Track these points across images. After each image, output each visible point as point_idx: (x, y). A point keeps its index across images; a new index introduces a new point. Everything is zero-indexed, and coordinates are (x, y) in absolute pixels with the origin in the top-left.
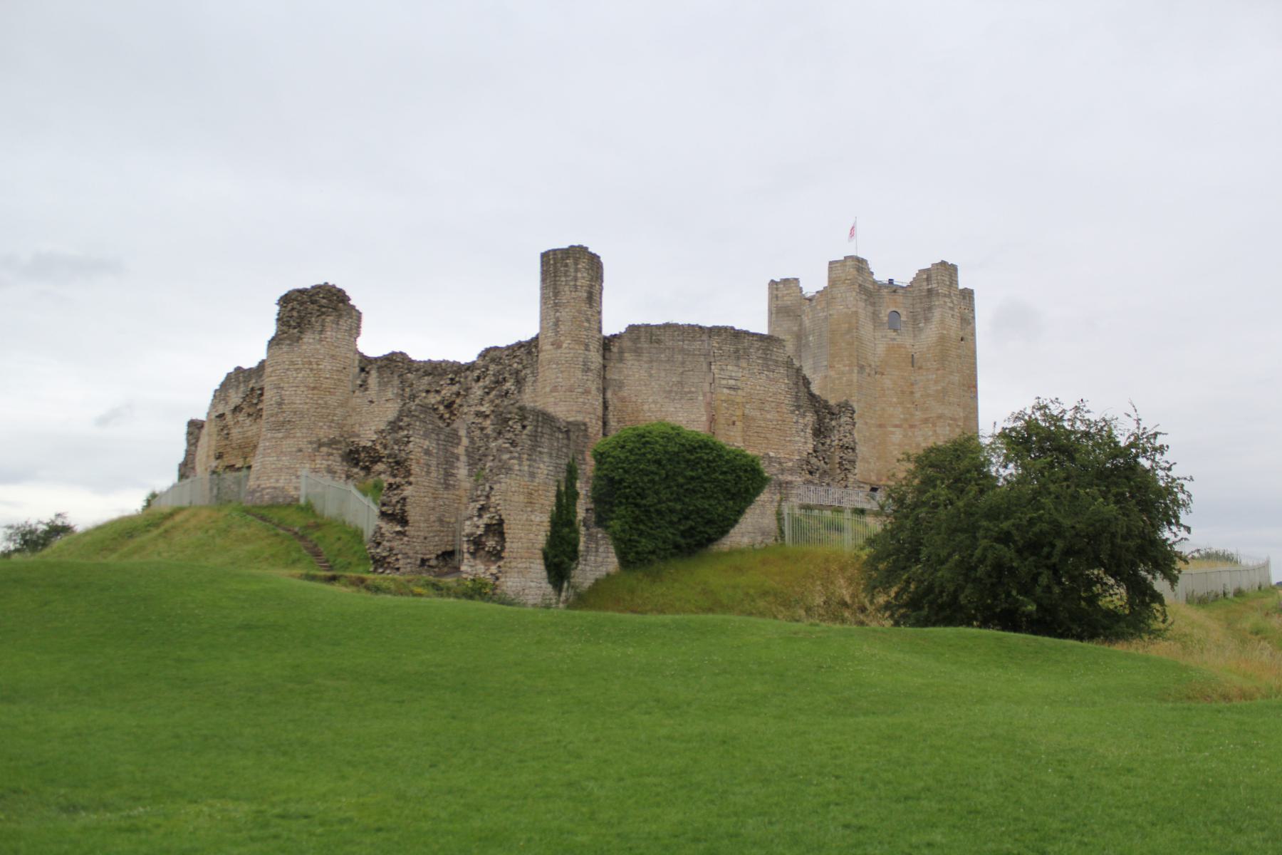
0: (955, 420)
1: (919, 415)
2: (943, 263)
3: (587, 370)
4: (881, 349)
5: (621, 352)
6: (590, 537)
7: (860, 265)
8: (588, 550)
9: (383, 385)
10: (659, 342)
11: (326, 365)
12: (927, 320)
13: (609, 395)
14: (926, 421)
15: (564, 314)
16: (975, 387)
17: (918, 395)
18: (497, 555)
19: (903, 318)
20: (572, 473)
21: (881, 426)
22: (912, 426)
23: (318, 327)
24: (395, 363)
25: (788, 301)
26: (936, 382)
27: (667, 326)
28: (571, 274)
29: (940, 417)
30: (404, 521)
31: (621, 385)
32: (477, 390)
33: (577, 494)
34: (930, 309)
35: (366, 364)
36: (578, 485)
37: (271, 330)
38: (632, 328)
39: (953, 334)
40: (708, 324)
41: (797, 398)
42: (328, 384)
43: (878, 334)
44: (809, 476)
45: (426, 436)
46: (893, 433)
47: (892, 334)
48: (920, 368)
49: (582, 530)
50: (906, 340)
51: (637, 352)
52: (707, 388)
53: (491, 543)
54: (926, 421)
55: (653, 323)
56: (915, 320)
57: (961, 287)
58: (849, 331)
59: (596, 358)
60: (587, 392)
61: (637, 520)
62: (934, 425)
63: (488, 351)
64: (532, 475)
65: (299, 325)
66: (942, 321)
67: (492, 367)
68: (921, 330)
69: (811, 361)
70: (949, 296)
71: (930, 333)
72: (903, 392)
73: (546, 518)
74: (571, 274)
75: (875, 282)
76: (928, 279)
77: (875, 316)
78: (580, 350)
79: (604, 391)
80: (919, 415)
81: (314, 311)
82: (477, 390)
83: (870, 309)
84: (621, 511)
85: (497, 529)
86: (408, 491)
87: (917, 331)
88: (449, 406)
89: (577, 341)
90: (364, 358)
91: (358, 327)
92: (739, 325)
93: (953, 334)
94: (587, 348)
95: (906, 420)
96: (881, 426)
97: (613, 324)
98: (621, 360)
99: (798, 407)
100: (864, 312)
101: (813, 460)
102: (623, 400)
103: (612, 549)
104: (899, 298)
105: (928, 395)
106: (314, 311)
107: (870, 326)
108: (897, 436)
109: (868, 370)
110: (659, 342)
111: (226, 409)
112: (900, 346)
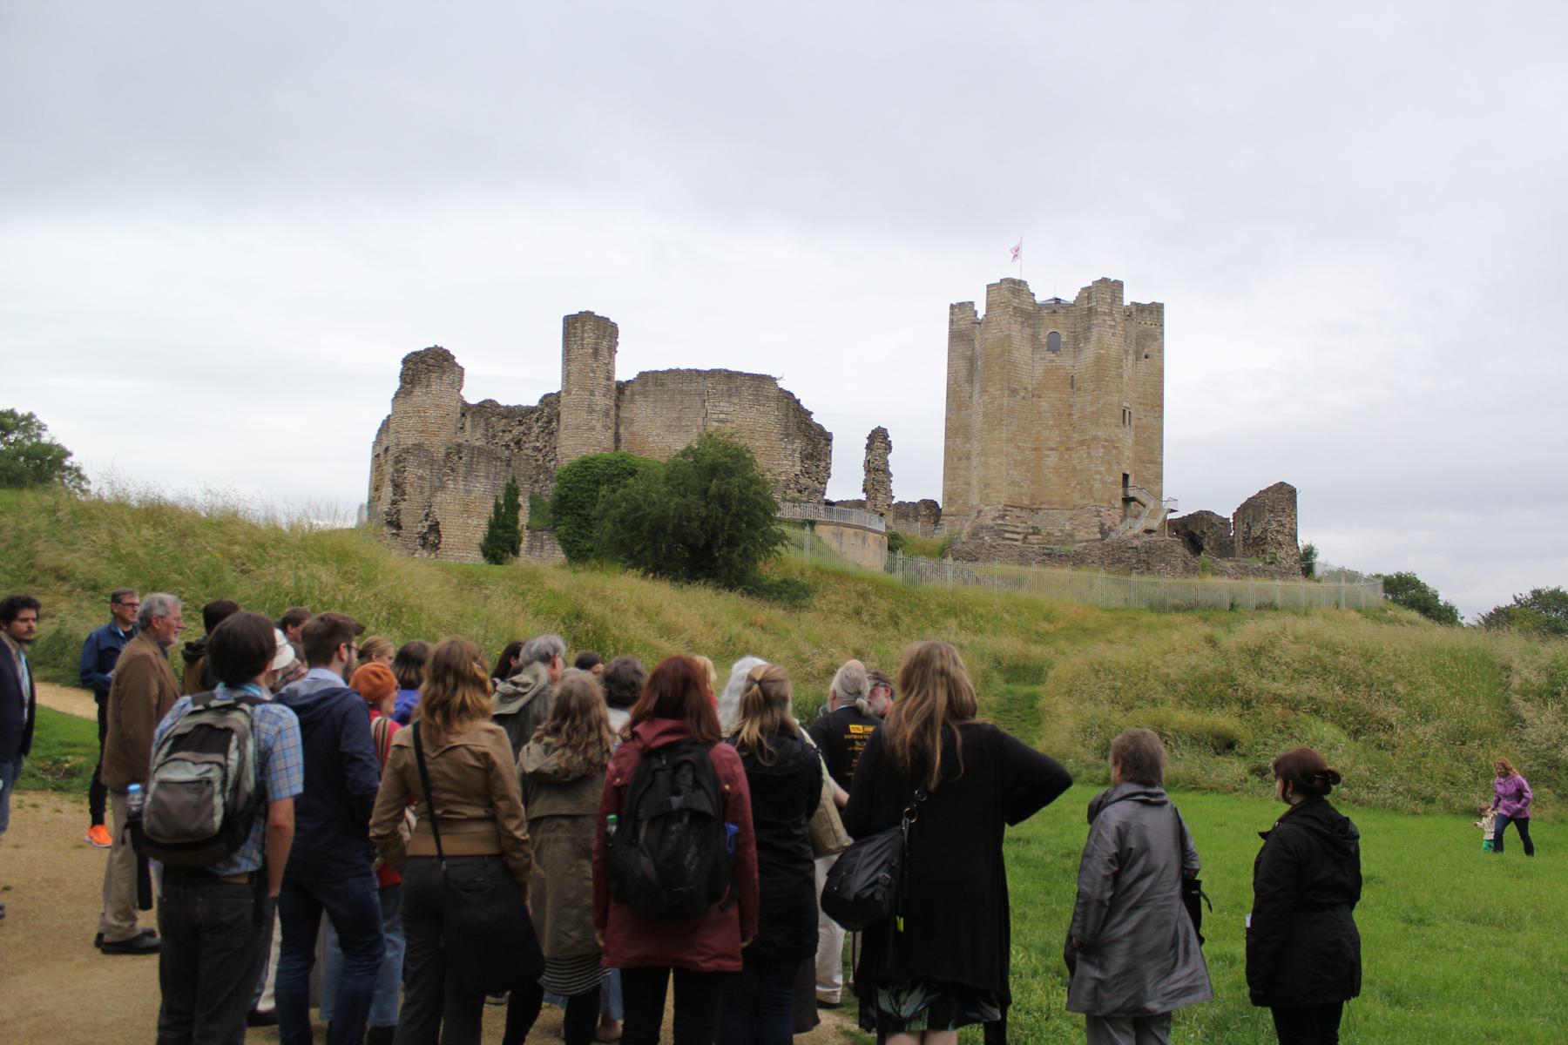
0: (1112, 441)
2: (1104, 280)
3: (591, 410)
4: (1039, 371)
5: (633, 395)
6: (534, 537)
7: (1017, 287)
8: (531, 548)
9: (474, 426)
10: (663, 385)
11: (432, 413)
12: (1087, 339)
13: (622, 430)
14: (1082, 443)
15: (574, 368)
16: (1161, 406)
18: (436, 547)
19: (1064, 339)
20: (512, 492)
21: (1036, 449)
22: (1068, 449)
23: (425, 382)
24: (487, 409)
25: (963, 325)
26: (1092, 403)
27: (670, 371)
28: (588, 335)
29: (1094, 439)
30: (398, 527)
31: (632, 422)
32: (536, 430)
33: (519, 506)
34: (1089, 328)
35: (466, 409)
36: (520, 499)
37: (396, 384)
38: (642, 375)
39: (1113, 353)
40: (705, 366)
41: (787, 427)
42: (433, 428)
43: (1037, 356)
44: (797, 495)
45: (419, 466)
47: (1051, 356)
49: (526, 534)
50: (1066, 361)
51: (645, 394)
52: (700, 421)
53: (432, 538)
54: (1082, 443)
55: (661, 369)
57: (1127, 302)
58: (1002, 354)
59: (603, 401)
60: (592, 429)
61: (579, 526)
63: (546, 396)
64: (469, 492)
65: (412, 382)
66: (1099, 341)
67: (547, 410)
68: (1081, 350)
70: (1111, 314)
71: (1089, 353)
72: (1060, 414)
73: (484, 524)
74: (588, 335)
75: (1035, 303)
76: (1089, 298)
77: (1034, 338)
78: (586, 395)
79: (617, 426)
81: (428, 368)
82: (536, 430)
83: (1029, 331)
84: (567, 519)
85: (435, 528)
86: (403, 505)
87: (1077, 350)
88: (518, 443)
89: (583, 388)
90: (465, 404)
91: (461, 380)
92: (733, 368)
93: (1113, 353)
94: (592, 393)
96: (1036, 449)
97: (625, 369)
98: (632, 401)
99: (787, 435)
100: (1018, 333)
101: (804, 481)
102: (632, 434)
103: (559, 547)
104: (1060, 318)
106: (428, 368)
107: (1028, 349)
108: (1052, 459)
109: (1022, 393)
110: (663, 385)
111: (380, 450)
112: (1059, 368)
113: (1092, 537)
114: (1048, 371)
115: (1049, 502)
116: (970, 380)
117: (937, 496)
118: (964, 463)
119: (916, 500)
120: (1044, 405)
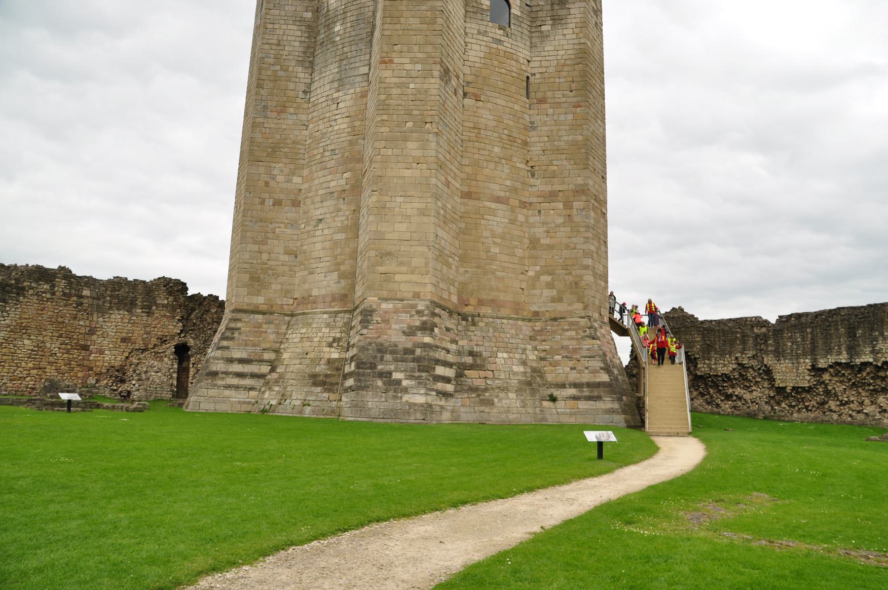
1: (540, 185)
4: (476, 53)
12: (557, 20)
14: (552, 196)
17: (536, 149)
21: (467, 195)
22: (524, 205)
43: (472, 27)
46: (493, 212)
48: (542, 101)
54: (552, 196)
56: (533, 20)
62: (568, 205)
68: (544, 37)
69: (334, 68)
80: (540, 185)
95: (514, 190)
105: (558, 151)
108: (498, 220)
112: (509, 56)
113: (586, 378)
114: (490, 55)
115: (493, 302)
116: (309, 61)
117: (208, 275)
118: (289, 213)
119: (148, 276)
120: (486, 117)
